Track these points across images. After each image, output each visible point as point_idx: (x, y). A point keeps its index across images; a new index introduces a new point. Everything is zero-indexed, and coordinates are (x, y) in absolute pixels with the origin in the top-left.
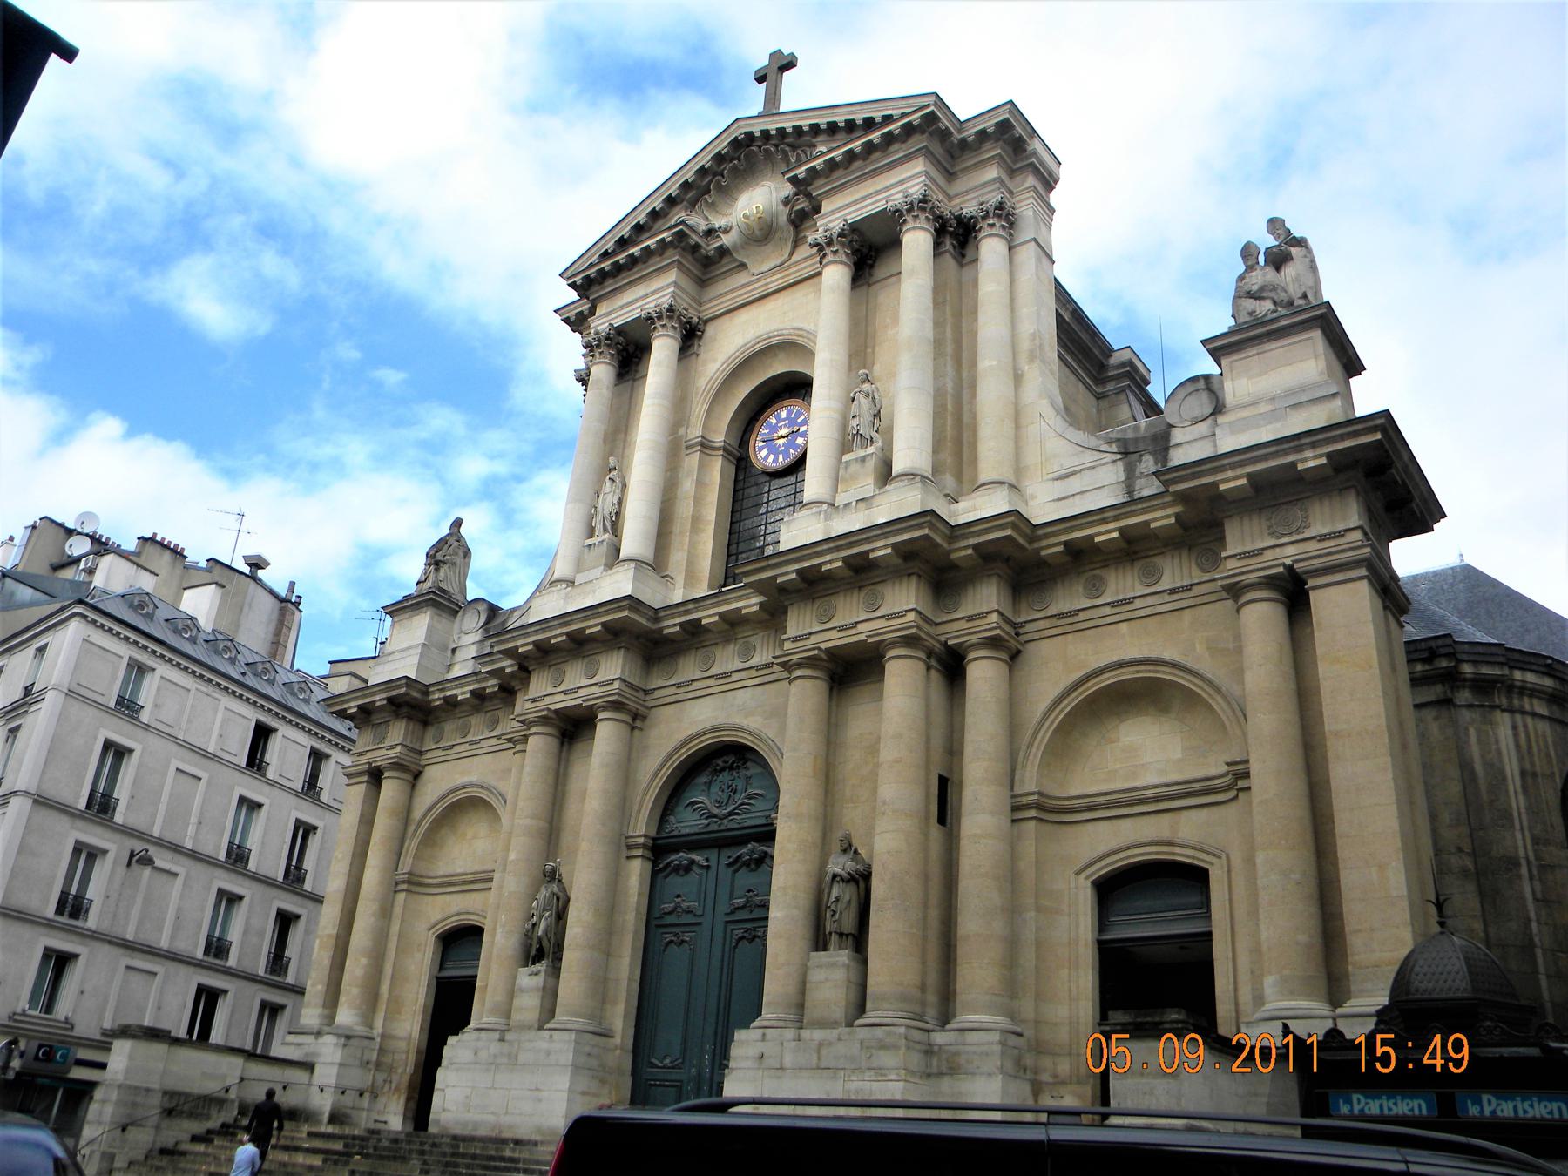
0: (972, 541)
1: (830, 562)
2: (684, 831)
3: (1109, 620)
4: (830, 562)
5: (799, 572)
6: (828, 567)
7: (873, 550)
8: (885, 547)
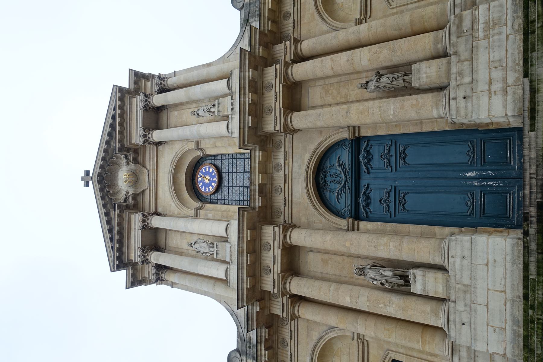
0: (257, 46)
1: (249, 98)
2: (349, 203)
3: (299, 7)
4: (249, 98)
5: (249, 115)
6: (250, 100)
7: (249, 77)
8: (249, 71)
